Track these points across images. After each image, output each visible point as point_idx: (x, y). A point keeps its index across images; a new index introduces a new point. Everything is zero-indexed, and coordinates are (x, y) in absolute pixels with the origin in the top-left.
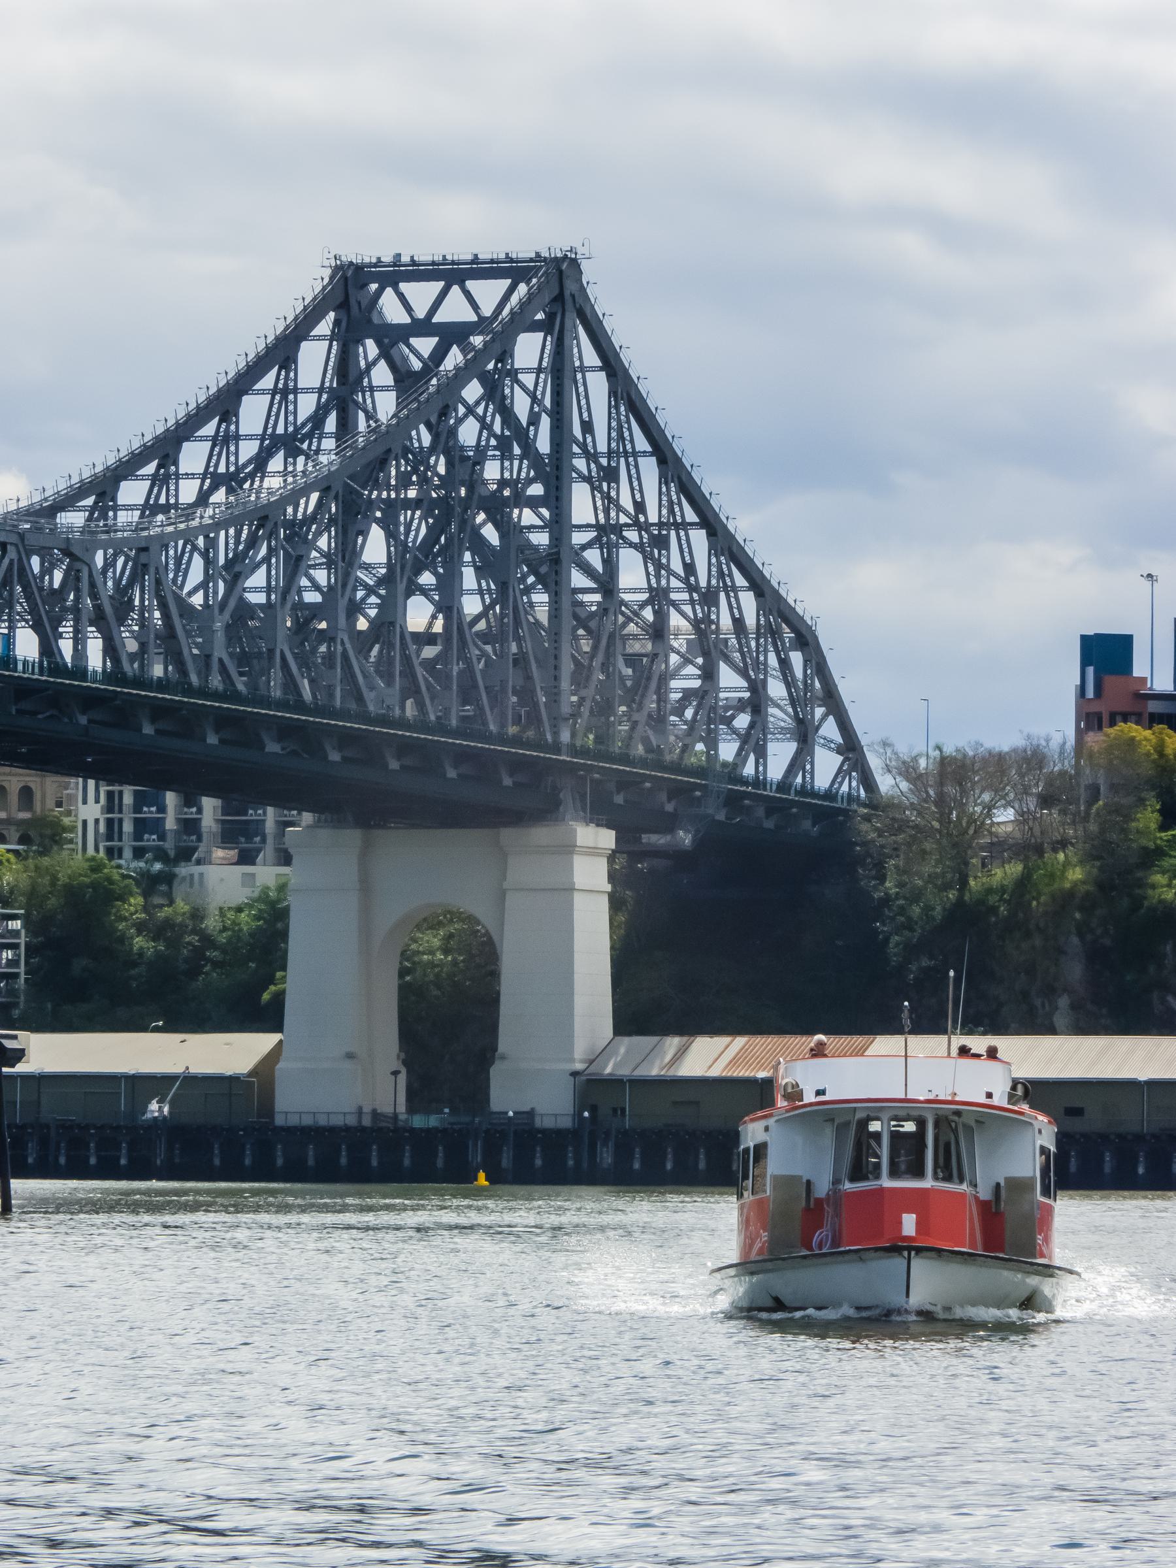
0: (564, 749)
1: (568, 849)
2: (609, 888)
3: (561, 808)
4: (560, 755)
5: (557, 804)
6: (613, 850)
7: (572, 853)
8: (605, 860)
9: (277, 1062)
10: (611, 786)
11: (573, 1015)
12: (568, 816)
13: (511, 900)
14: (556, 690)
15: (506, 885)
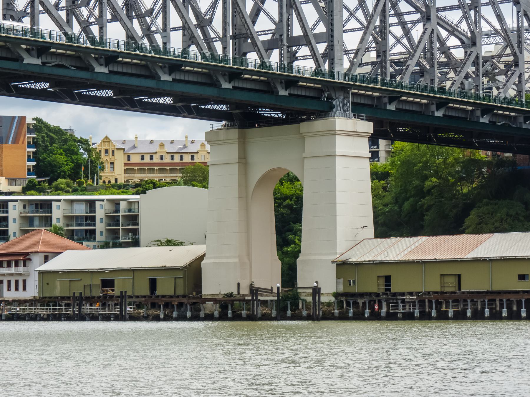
0: (327, 75)
1: (333, 132)
2: (370, 155)
3: (334, 110)
4: (325, 78)
5: (331, 107)
6: (372, 134)
7: (335, 134)
8: (367, 139)
9: (203, 259)
10: (386, 100)
11: (335, 228)
12: (338, 113)
13: (306, 161)
14: (332, 44)
15: (304, 155)
